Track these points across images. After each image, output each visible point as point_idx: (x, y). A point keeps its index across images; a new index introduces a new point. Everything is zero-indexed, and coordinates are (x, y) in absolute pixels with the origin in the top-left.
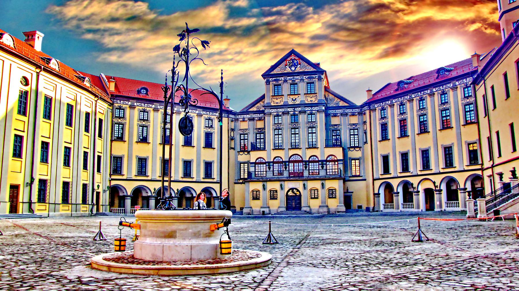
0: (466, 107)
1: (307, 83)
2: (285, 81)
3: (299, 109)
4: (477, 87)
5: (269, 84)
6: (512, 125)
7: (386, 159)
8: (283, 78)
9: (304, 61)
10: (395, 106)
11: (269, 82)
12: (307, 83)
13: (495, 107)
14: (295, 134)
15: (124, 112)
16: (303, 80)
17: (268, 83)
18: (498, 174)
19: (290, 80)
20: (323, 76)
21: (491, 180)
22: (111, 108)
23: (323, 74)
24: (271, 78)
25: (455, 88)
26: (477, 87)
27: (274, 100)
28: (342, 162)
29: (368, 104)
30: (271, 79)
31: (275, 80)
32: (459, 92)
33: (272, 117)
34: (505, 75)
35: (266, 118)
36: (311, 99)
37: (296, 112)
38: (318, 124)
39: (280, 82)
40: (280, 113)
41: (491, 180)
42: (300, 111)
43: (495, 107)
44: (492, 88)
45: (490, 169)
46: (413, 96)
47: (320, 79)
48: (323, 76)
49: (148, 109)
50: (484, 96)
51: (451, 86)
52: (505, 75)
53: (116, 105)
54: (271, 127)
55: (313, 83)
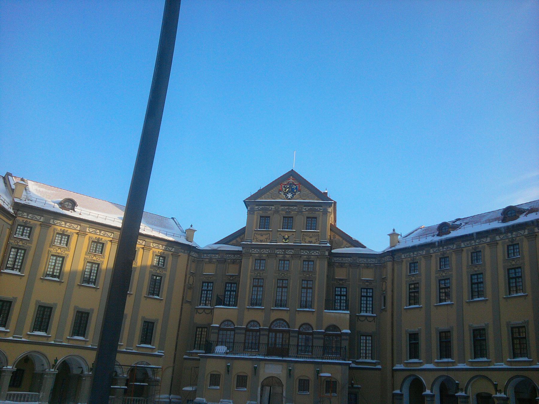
1: (307, 218)
2: (277, 212)
3: (291, 252)
5: (253, 214)
7: (414, 337)
8: (273, 207)
9: (307, 187)
11: (254, 211)
12: (307, 218)
14: (282, 287)
15: (30, 231)
16: (302, 212)
17: (250, 212)
19: (283, 210)
20: (330, 210)
22: (10, 222)
23: (330, 206)
24: (257, 205)
27: (258, 236)
28: (348, 337)
29: (392, 254)
30: (256, 207)
31: (262, 209)
33: (251, 260)
35: (243, 260)
36: (311, 240)
37: (288, 256)
38: (317, 276)
39: (269, 212)
40: (264, 255)
42: (292, 256)
47: (325, 212)
48: (330, 210)
49: (69, 230)
53: (20, 219)
54: (249, 274)
55: (316, 218)
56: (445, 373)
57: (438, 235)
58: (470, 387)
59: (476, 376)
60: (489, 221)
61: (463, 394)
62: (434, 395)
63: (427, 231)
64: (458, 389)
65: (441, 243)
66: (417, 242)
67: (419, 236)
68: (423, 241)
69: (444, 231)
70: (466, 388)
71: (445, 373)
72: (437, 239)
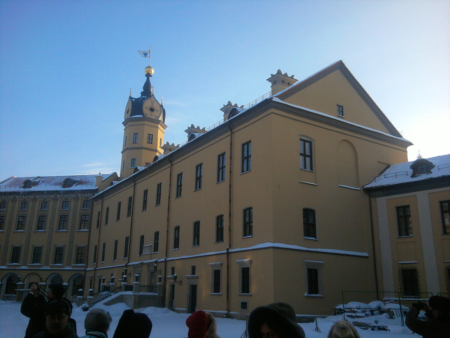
0: (83, 217)
4: (95, 203)
6: (116, 242)
10: (17, 202)
13: (106, 223)
18: (98, 277)
21: (91, 280)
25: (76, 199)
26: (95, 203)
32: (80, 203)
34: (120, 204)
41: (91, 280)
43: (106, 223)
44: (108, 209)
45: (93, 271)
46: (37, 197)
50: (99, 213)
51: (74, 196)
52: (120, 204)
56: (13, 272)
57: (23, 187)
58: (26, 279)
59: (32, 273)
60: (56, 184)
61: (21, 283)
62: (3, 284)
63: (16, 181)
64: (19, 280)
65: (24, 193)
66: (8, 190)
67: (11, 185)
68: (13, 189)
69: (27, 185)
70: (24, 280)
71: (13, 272)
72: (22, 190)
